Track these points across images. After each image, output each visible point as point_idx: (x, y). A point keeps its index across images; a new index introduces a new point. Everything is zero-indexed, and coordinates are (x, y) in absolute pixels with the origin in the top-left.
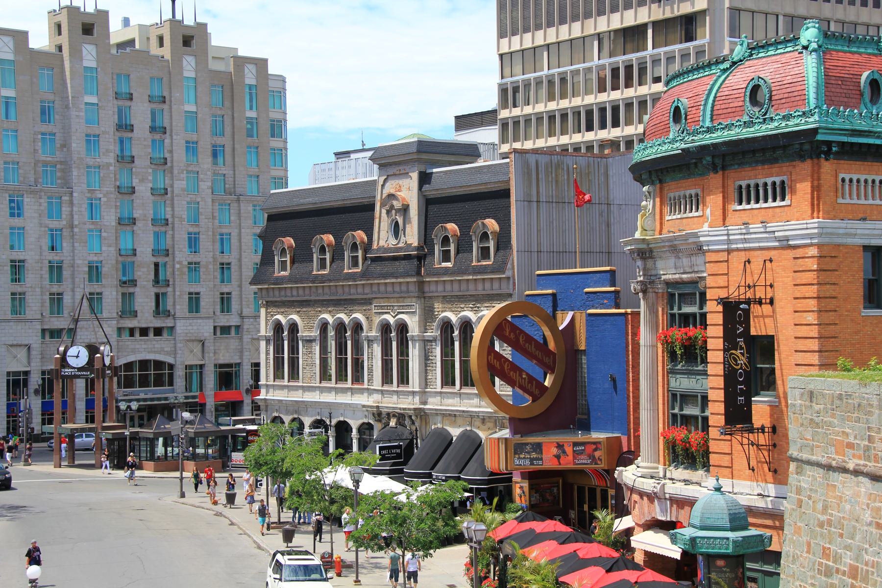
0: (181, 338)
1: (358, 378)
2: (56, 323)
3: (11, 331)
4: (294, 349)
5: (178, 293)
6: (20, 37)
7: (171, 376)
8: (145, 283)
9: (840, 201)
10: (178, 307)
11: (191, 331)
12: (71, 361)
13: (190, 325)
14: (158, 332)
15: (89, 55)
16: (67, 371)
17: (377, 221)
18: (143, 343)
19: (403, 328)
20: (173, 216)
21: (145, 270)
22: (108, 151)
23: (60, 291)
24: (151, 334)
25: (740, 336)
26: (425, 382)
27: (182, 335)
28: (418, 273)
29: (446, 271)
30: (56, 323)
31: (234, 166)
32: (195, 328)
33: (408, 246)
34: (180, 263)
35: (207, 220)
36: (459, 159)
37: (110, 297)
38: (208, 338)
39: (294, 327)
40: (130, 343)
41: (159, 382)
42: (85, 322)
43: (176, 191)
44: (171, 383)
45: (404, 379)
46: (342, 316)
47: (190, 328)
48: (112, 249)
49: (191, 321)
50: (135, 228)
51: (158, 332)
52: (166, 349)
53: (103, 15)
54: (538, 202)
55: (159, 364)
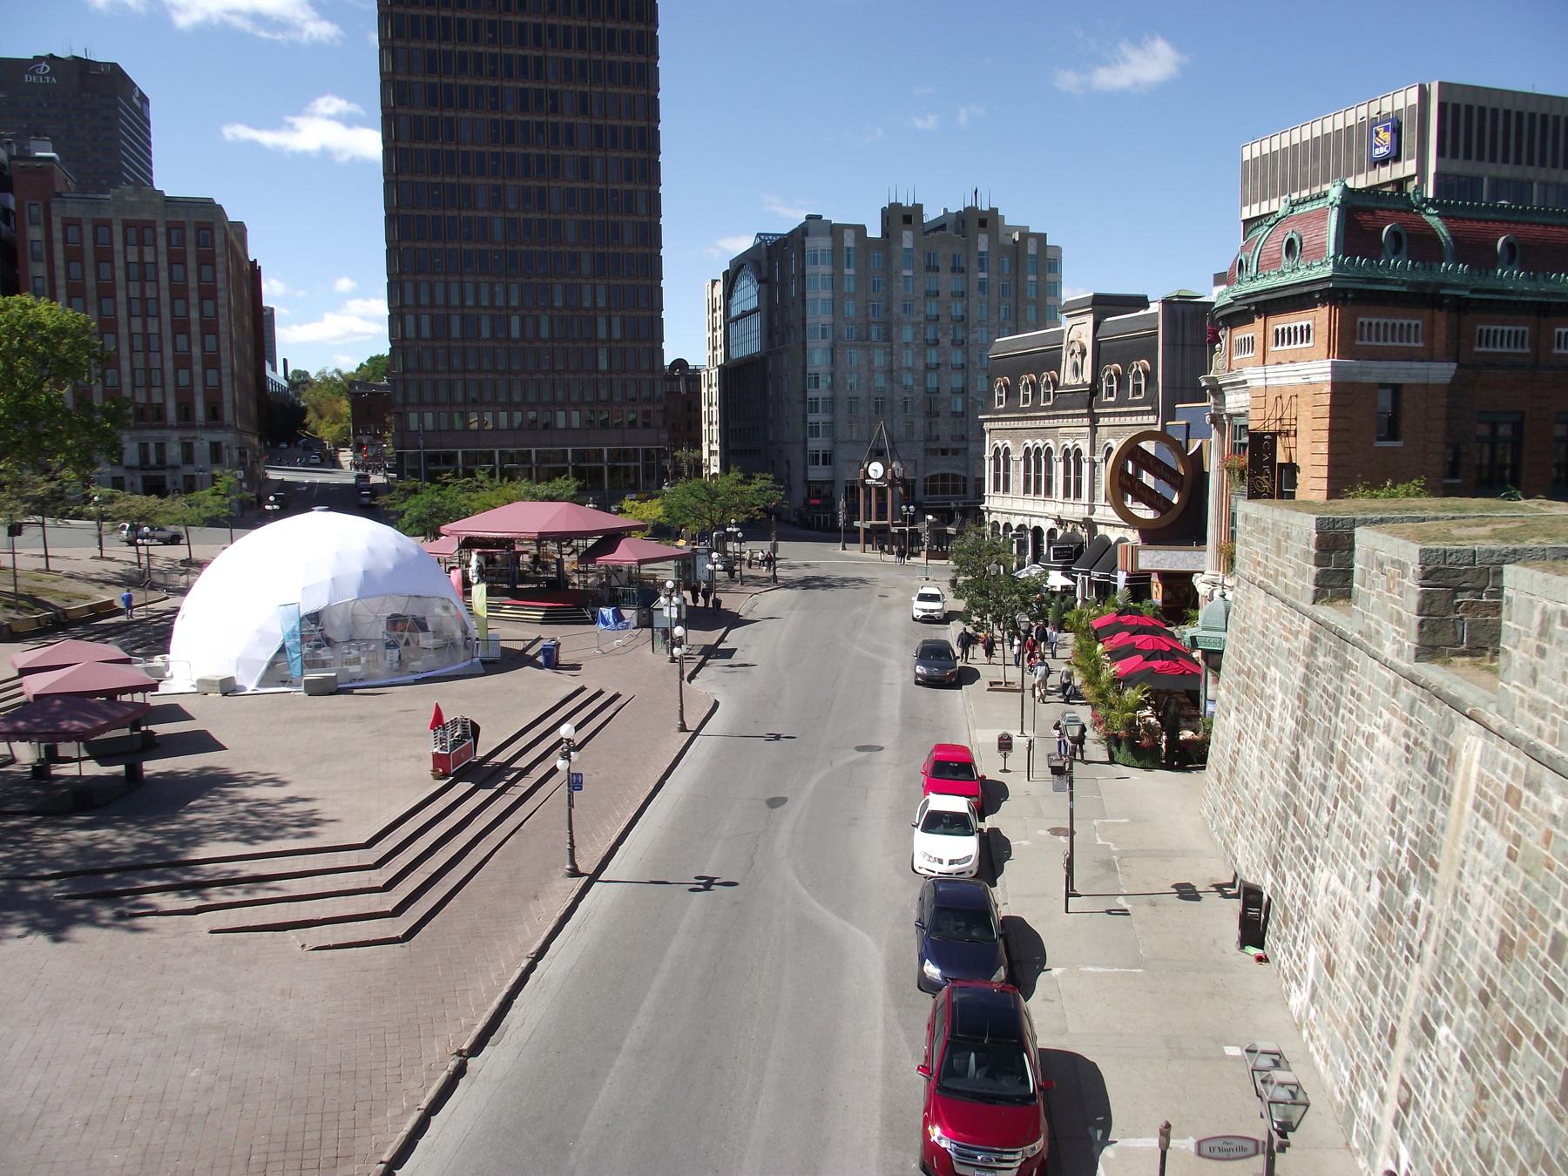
1: (1048, 492)
4: (1007, 468)
5: (970, 422)
6: (860, 229)
7: (965, 486)
9: (1358, 342)
10: (970, 433)
12: (871, 473)
14: (956, 452)
15: (907, 239)
16: (868, 481)
17: (1063, 363)
19: (1078, 452)
20: (968, 362)
22: (919, 312)
24: (950, 454)
25: (1266, 463)
26: (1092, 497)
28: (1090, 406)
29: (1110, 405)
31: (1017, 320)
33: (1084, 383)
34: (972, 398)
36: (1123, 309)
39: (1007, 451)
41: (955, 490)
43: (971, 342)
44: (965, 492)
45: (1078, 494)
46: (1039, 441)
48: (921, 388)
51: (956, 452)
53: (918, 208)
54: (1183, 345)
55: (955, 477)
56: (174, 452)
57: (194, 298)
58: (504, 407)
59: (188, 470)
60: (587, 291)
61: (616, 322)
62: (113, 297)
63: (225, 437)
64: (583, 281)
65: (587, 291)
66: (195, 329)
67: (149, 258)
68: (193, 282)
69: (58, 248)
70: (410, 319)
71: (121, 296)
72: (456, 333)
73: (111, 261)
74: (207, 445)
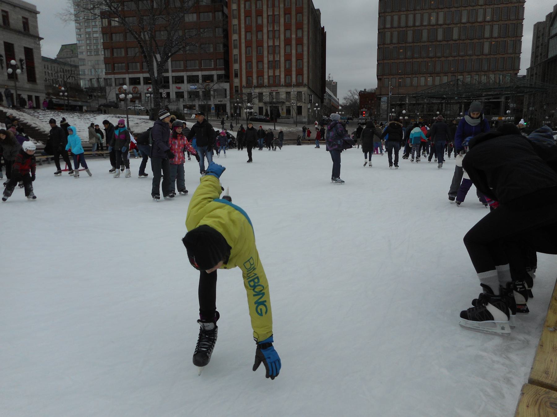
56: (283, 96)
57: (294, 28)
58: (431, 74)
59: (288, 104)
60: (481, 12)
61: (496, 28)
62: (262, 31)
63: (304, 90)
64: (479, 7)
65: (481, 12)
66: (294, 42)
67: (276, 13)
68: (293, 21)
69: (242, 11)
70: (388, 35)
71: (265, 30)
72: (410, 39)
73: (262, 16)
74: (296, 93)
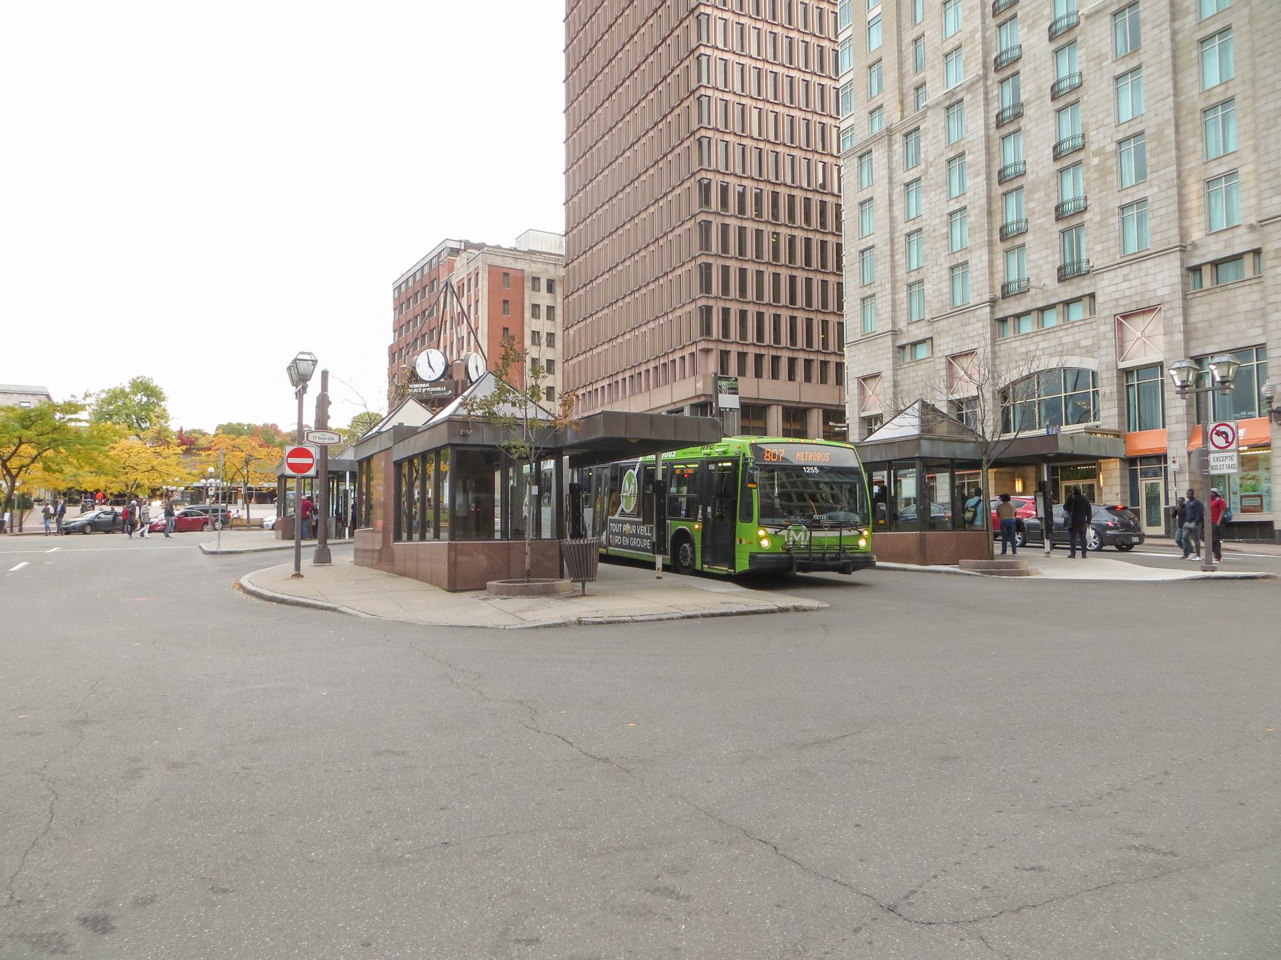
0: (1106, 313)
2: (917, 332)
3: (861, 357)
8: (1043, 220)
11: (1128, 293)
13: (1126, 279)
18: (1040, 338)
21: (1042, 194)
23: (920, 277)
27: (1107, 305)
30: (917, 332)
32: (1134, 283)
35: (1157, 31)
37: (978, 267)
38: (1167, 299)
40: (1017, 343)
42: (945, 321)
47: (1126, 285)
49: (1126, 270)
50: (1023, 122)
52: (1083, 343)
